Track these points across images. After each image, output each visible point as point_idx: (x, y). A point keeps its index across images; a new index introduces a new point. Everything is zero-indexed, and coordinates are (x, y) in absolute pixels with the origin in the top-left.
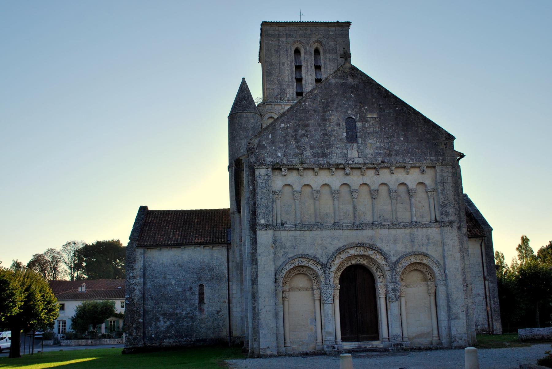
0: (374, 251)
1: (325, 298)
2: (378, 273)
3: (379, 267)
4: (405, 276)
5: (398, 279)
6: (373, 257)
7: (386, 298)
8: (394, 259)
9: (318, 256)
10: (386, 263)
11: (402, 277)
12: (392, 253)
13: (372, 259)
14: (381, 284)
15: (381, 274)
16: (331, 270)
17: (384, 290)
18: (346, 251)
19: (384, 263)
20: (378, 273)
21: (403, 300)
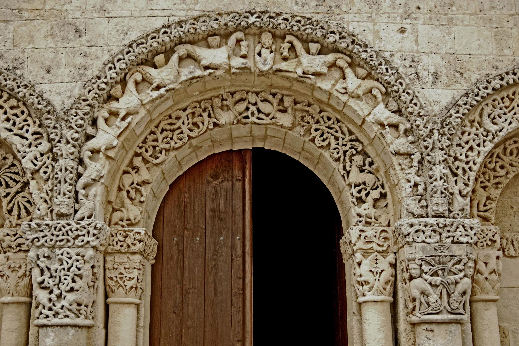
0: (330, 57)
1: (42, 296)
2: (355, 177)
3: (357, 147)
4: (495, 193)
5: (459, 202)
6: (325, 85)
7: (394, 306)
8: (437, 98)
9: (31, 72)
10: (395, 118)
11: (482, 195)
12: (428, 63)
13: (325, 103)
14: (370, 231)
15: (369, 179)
16: (92, 144)
17: (384, 264)
18: (182, 50)
19: (382, 113)
20: (355, 177)
21: (489, 318)
